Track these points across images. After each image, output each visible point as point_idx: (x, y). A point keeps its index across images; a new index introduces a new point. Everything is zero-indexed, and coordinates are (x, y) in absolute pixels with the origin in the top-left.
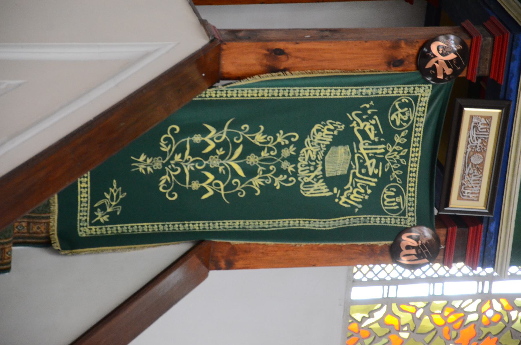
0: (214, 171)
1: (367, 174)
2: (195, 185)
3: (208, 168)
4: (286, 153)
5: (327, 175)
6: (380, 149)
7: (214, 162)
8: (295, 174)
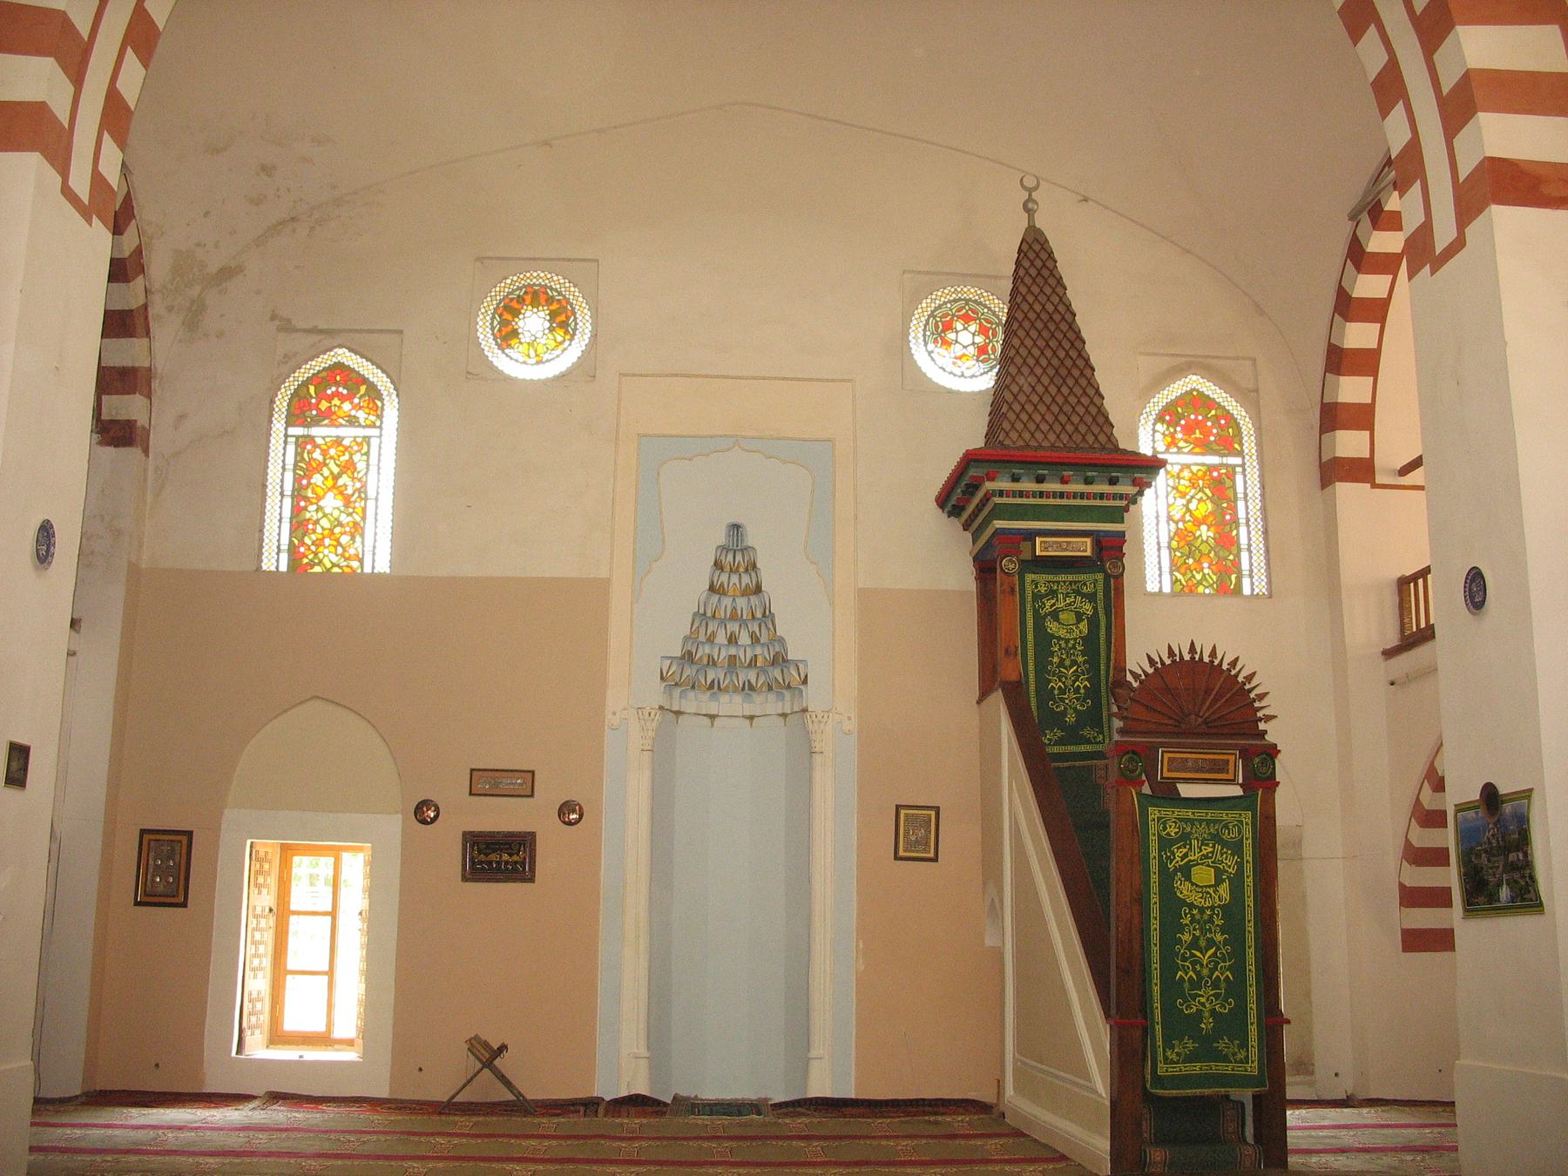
0: (1212, 971)
2: (1223, 985)
7: (1205, 972)
8: (1212, 908)
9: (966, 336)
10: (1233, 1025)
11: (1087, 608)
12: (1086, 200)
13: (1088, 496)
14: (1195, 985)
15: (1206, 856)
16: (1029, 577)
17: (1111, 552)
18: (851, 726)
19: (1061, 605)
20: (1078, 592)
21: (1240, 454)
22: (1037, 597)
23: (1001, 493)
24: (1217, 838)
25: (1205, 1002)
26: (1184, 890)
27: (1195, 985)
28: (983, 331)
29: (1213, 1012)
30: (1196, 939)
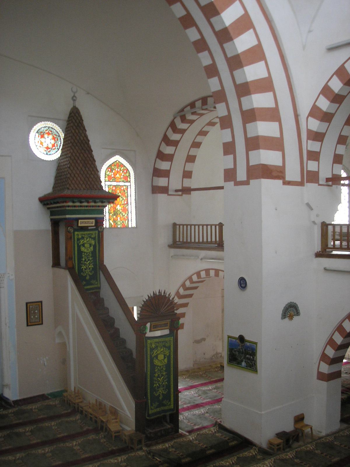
1: (163, 350)
3: (162, 384)
4: (159, 369)
5: (163, 358)
6: (159, 348)
7: (161, 383)
8: (163, 366)
9: (48, 141)
10: (167, 397)
11: (93, 242)
12: (88, 93)
13: (96, 206)
14: (158, 387)
15: (162, 352)
16: (76, 233)
17: (99, 222)
18: (13, 277)
19: (85, 241)
20: (90, 237)
21: (130, 182)
22: (78, 239)
23: (69, 206)
24: (164, 346)
25: (161, 391)
26: (156, 362)
27: (158, 387)
28: (54, 138)
29: (163, 394)
30: (159, 375)
